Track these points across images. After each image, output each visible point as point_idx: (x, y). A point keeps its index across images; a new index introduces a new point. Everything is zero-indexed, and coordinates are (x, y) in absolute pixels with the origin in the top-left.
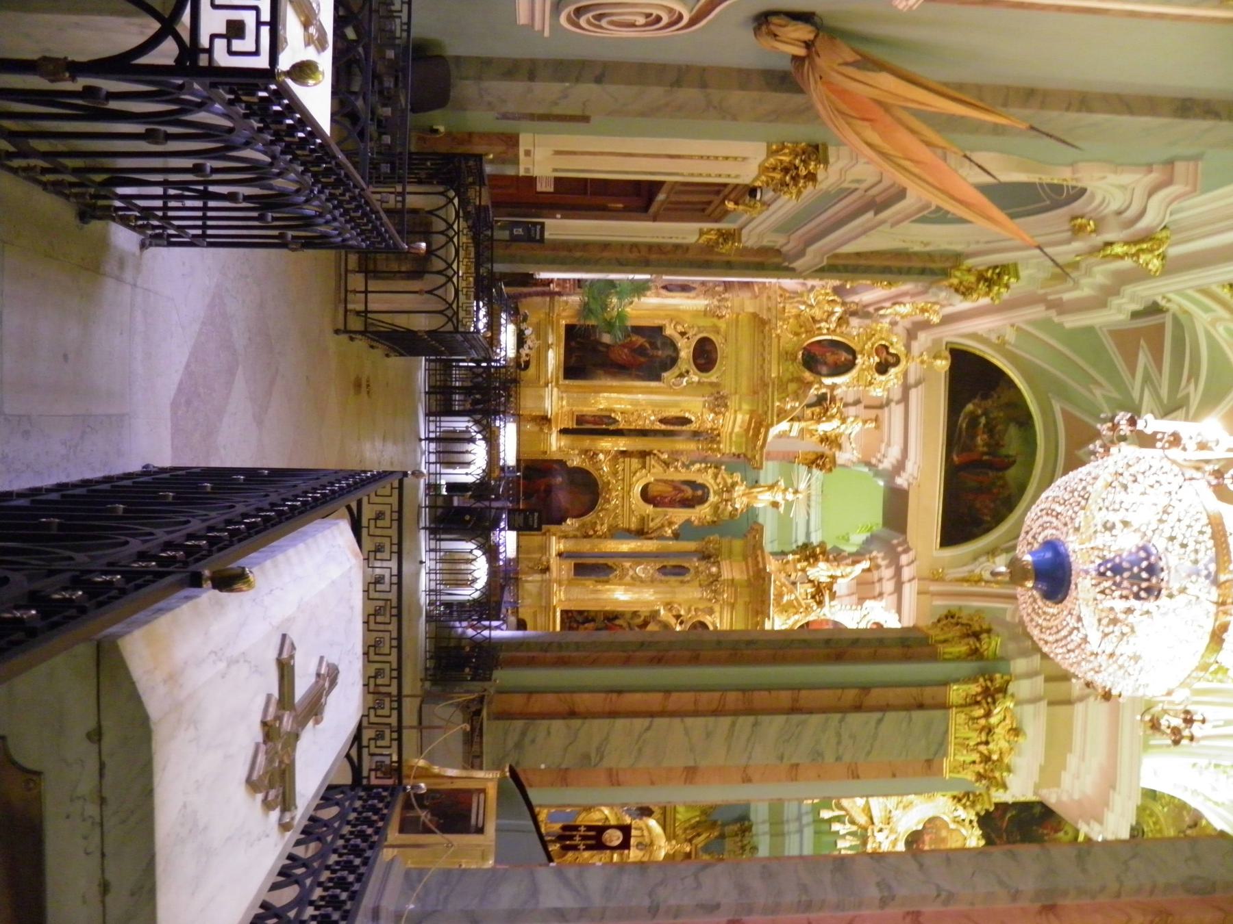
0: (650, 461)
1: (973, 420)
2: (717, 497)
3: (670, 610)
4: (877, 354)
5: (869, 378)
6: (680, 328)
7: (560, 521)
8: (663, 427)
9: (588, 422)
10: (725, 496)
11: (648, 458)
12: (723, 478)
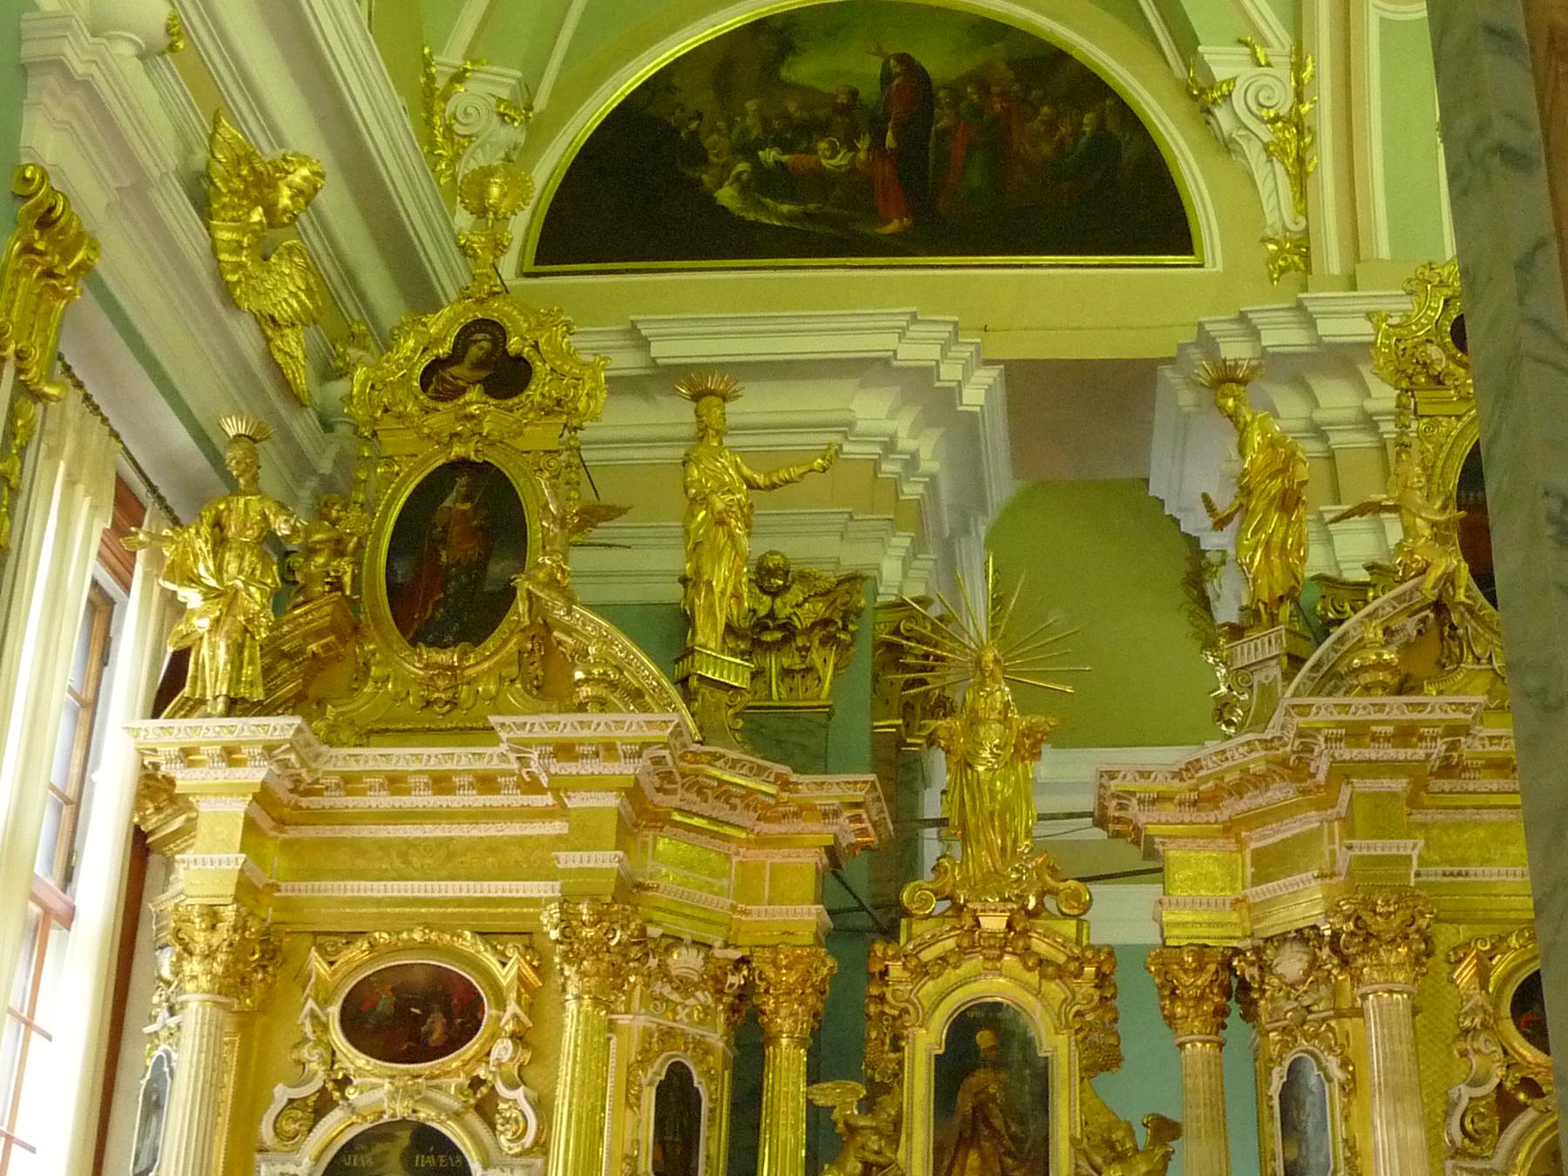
1: (767, 183)
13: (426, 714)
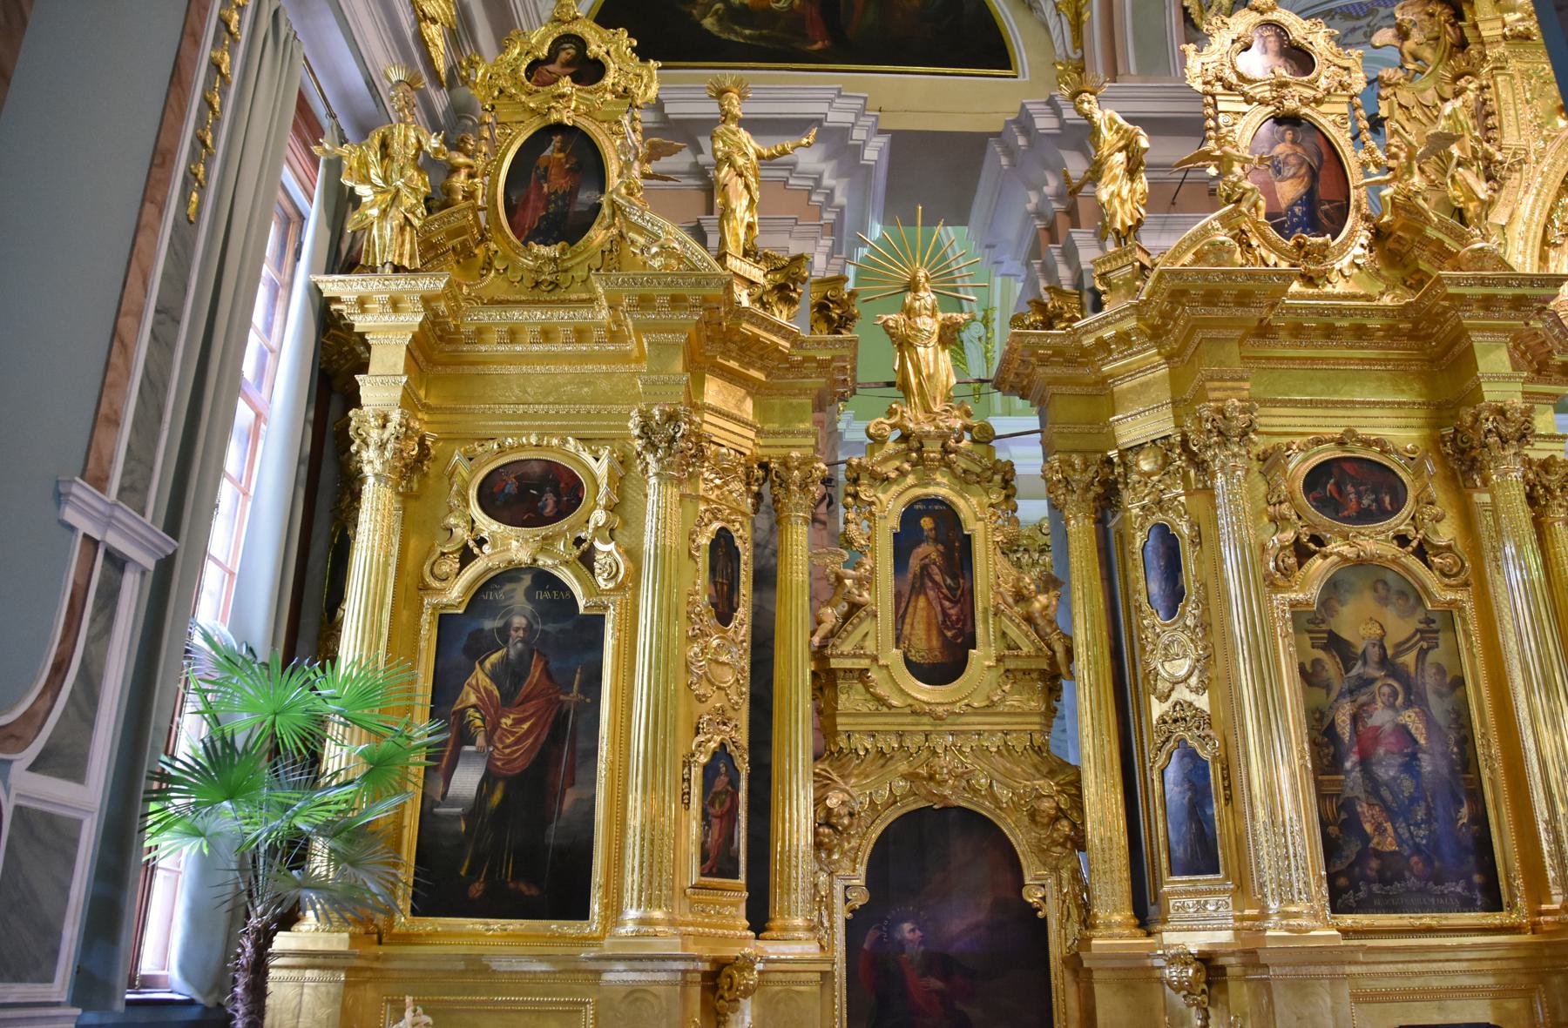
3: (1286, 572)
4: (556, 81)
5: (609, 97)
8: (743, 613)
9: (730, 838)
10: (933, 450)
11: (835, 663)
12: (886, 460)
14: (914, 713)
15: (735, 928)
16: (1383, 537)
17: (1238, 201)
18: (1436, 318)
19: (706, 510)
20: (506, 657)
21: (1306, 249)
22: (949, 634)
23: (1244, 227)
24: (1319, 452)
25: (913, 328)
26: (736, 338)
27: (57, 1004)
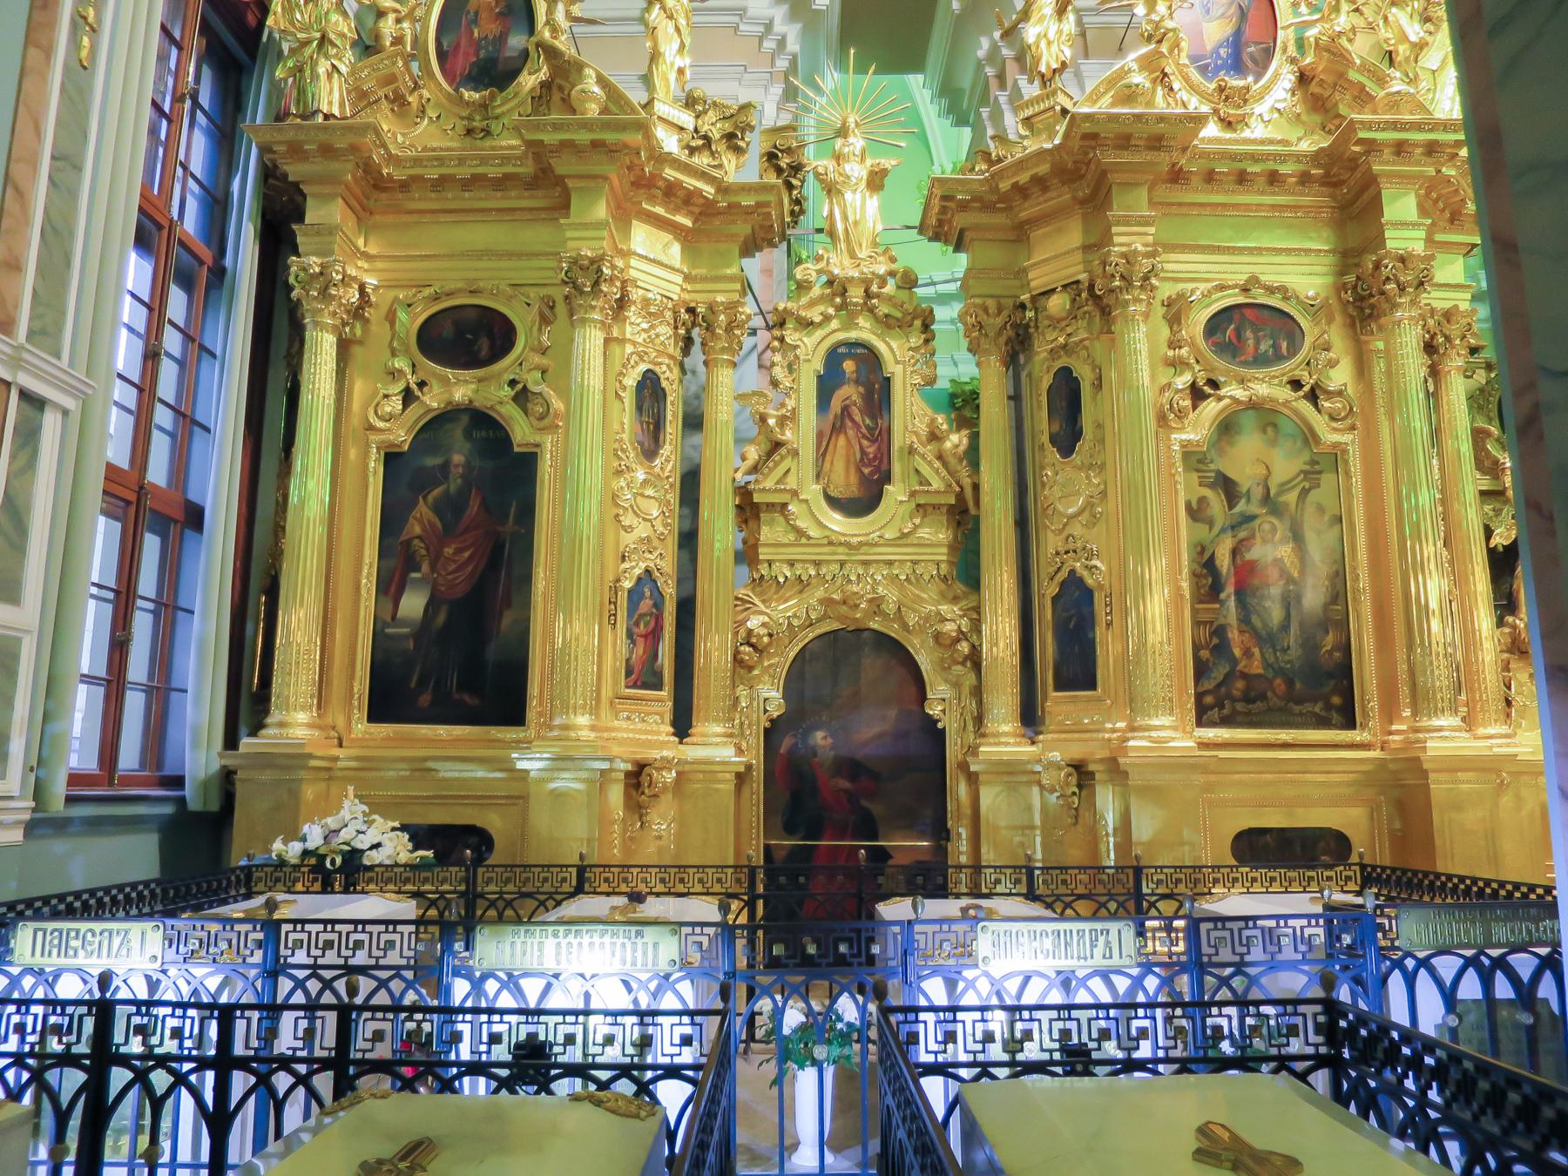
0: (766, 488)
2: (861, 321)
3: (1181, 414)
6: (396, 404)
7: (937, 737)
10: (856, 295)
11: (757, 498)
12: (812, 304)
13: (468, 139)
14: (831, 543)
15: (658, 733)
16: (1276, 381)
17: (1160, 41)
18: (1353, 163)
19: (633, 353)
20: (447, 492)
21: (1226, 93)
22: (866, 471)
23: (1167, 70)
24: (1222, 298)
25: (840, 174)
26: (661, 184)
27: (11, 798)
